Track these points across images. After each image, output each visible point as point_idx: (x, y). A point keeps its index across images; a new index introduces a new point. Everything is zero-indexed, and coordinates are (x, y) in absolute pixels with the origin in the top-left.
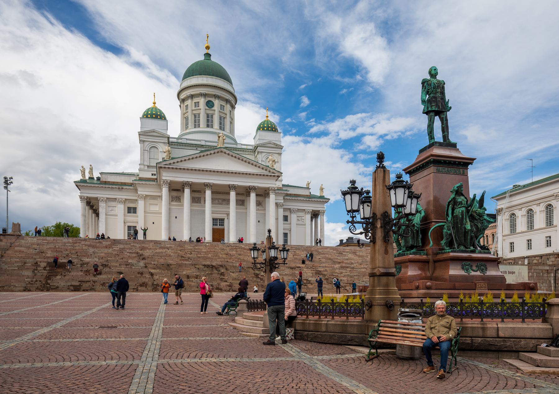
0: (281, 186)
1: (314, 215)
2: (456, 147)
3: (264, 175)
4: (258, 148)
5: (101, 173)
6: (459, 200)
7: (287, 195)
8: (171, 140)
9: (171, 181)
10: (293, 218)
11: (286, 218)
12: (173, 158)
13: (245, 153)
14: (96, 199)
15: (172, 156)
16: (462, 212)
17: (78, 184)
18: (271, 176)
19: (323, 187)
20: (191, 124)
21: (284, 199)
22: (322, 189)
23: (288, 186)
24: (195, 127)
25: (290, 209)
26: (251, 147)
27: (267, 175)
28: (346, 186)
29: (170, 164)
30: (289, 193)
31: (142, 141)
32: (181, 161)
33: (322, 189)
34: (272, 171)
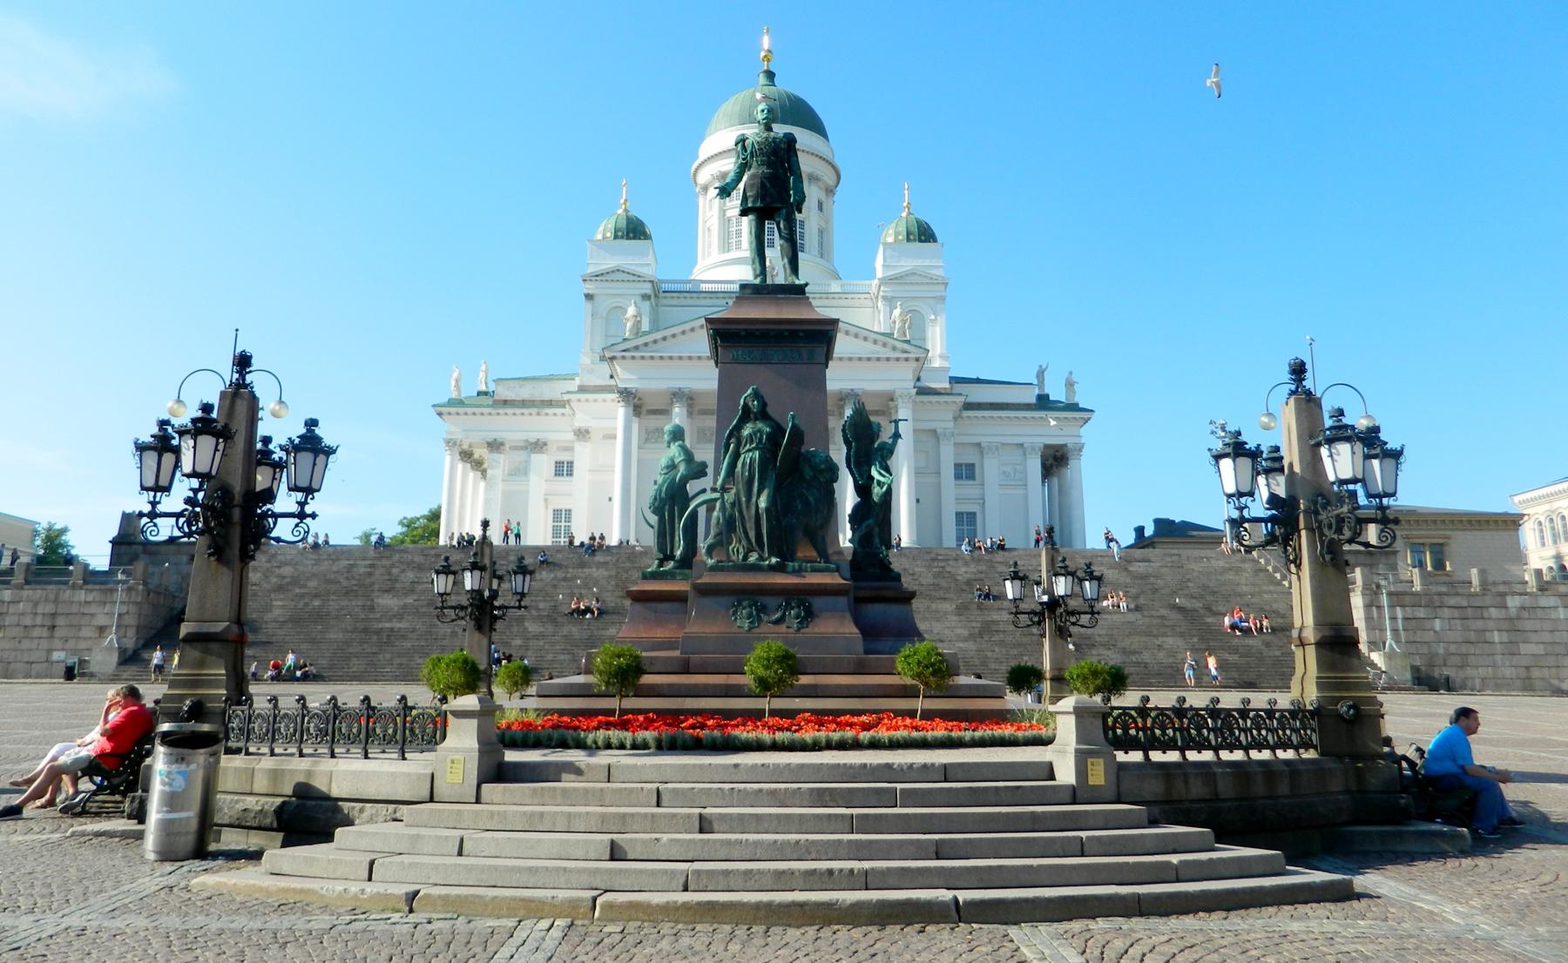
1: (1055, 458)
3: (878, 359)
5: (498, 381)
7: (969, 406)
10: (991, 469)
11: (965, 472)
13: (825, 302)
18: (898, 359)
19: (1075, 378)
21: (955, 419)
22: (1070, 384)
23: (978, 381)
25: (979, 445)
27: (888, 359)
29: (636, 348)
30: (972, 399)
31: (589, 297)
32: (664, 339)
33: (1070, 384)
34: (899, 345)
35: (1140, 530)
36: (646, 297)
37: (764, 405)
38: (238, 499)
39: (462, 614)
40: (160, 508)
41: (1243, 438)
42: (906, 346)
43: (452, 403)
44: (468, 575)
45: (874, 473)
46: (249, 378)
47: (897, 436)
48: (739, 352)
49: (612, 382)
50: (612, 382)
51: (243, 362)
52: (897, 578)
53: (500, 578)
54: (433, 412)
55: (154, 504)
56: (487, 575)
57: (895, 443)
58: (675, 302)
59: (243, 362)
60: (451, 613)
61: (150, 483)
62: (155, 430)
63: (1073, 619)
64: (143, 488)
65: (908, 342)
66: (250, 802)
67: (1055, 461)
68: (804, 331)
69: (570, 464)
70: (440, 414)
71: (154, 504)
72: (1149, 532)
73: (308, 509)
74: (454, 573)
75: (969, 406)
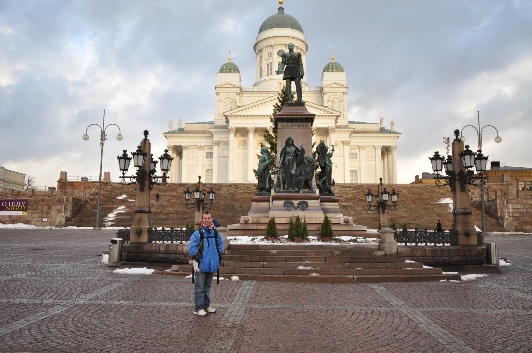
0: (347, 124)
2: (304, 105)
4: (324, 89)
6: (288, 150)
8: (244, 90)
9: (236, 128)
10: (363, 154)
12: (238, 107)
14: (181, 147)
15: (238, 105)
16: (289, 159)
17: (166, 135)
19: (393, 122)
20: (265, 73)
21: (350, 137)
22: (392, 124)
23: (358, 123)
24: (268, 75)
26: (318, 89)
27: (325, 116)
28: (121, 154)
29: (235, 113)
35: (417, 177)
36: (237, 94)
37: (293, 142)
38: (148, 172)
39: (193, 206)
40: (126, 175)
41: (439, 154)
42: (332, 111)
43: (169, 132)
44: (195, 193)
45: (327, 162)
46: (148, 138)
47: (333, 150)
48: (285, 124)
49: (226, 124)
50: (226, 124)
51: (146, 133)
52: (334, 195)
53: (204, 195)
54: (163, 135)
55: (124, 174)
56: (201, 194)
57: (333, 153)
58: (248, 95)
59: (146, 133)
60: (190, 206)
61: (123, 168)
62: (123, 153)
63: (388, 208)
64: (121, 170)
65: (333, 109)
66: (160, 255)
67: (386, 151)
68: (306, 118)
69: (212, 154)
70: (166, 137)
71: (124, 174)
72: (420, 177)
73: (167, 175)
74: (191, 193)
75: (355, 132)
